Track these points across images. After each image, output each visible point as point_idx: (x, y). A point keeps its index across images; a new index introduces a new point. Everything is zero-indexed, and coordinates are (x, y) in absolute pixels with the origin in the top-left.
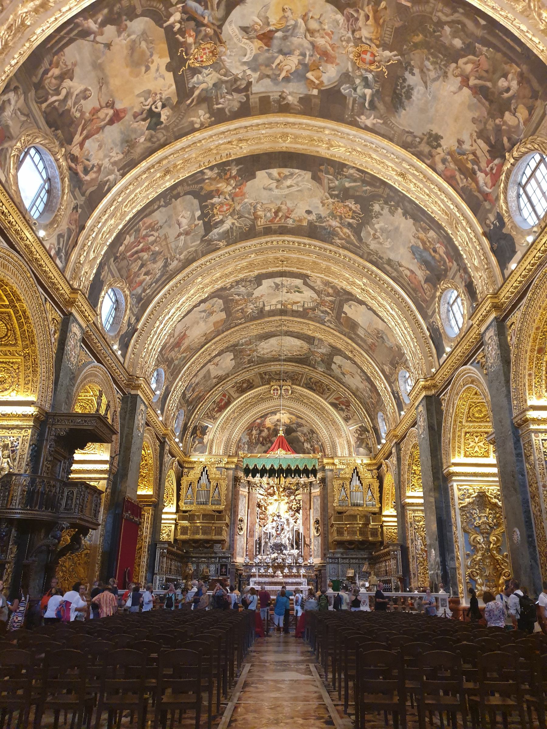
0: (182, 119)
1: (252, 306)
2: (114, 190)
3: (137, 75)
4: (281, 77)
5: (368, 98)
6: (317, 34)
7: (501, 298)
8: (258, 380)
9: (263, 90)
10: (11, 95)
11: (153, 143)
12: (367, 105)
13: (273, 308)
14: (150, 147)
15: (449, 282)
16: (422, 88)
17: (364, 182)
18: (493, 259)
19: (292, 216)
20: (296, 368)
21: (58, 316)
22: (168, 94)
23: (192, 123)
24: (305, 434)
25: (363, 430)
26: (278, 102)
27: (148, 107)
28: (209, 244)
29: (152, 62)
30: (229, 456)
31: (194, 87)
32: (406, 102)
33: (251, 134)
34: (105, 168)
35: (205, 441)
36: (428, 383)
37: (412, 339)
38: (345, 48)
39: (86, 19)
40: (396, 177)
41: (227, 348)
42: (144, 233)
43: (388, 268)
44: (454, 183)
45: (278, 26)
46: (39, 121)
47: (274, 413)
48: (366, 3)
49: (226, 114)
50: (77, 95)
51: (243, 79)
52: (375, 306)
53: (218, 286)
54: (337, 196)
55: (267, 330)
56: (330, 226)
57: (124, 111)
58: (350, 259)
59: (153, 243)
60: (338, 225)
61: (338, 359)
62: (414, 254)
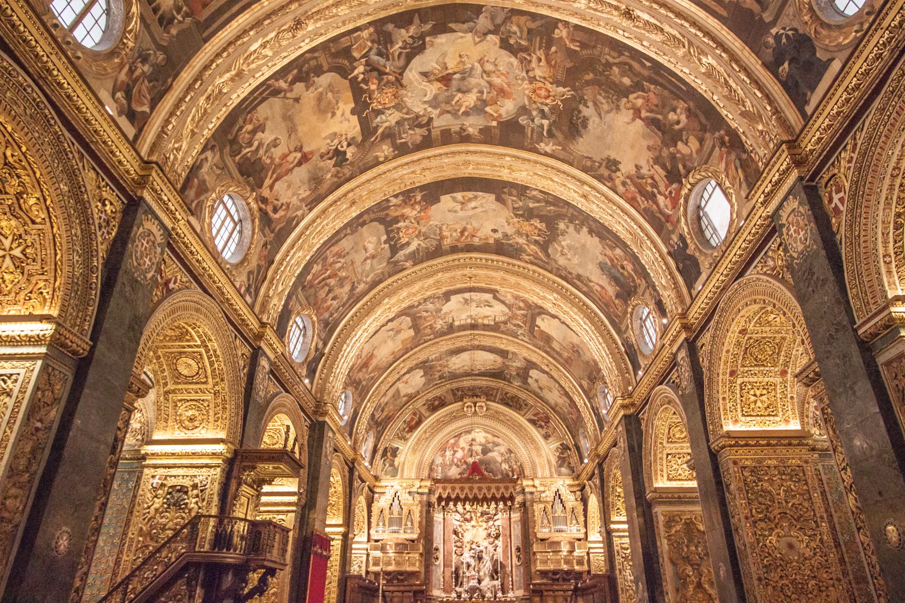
1: (441, 322)
2: (302, 224)
3: (324, 121)
4: (461, 112)
5: (545, 128)
7: (690, 317)
8: (450, 397)
9: (444, 123)
11: (339, 178)
12: (545, 133)
13: (463, 322)
15: (639, 299)
16: (597, 119)
17: (547, 202)
18: (680, 279)
19: (479, 234)
20: (490, 383)
21: (246, 350)
23: (377, 157)
24: (502, 454)
25: (565, 448)
26: (459, 133)
28: (395, 266)
29: (338, 108)
30: (422, 480)
32: (583, 131)
33: (434, 163)
35: (396, 463)
36: (627, 401)
37: (607, 355)
38: (520, 85)
40: (579, 199)
41: (417, 365)
42: (331, 260)
43: (578, 283)
44: (636, 204)
45: (456, 70)
47: (469, 432)
48: (537, 48)
51: (424, 116)
52: (568, 321)
53: (404, 305)
54: (521, 216)
55: (459, 344)
56: (517, 243)
57: (312, 153)
58: (539, 274)
59: (339, 269)
60: (525, 242)
61: (534, 373)
62: (602, 269)
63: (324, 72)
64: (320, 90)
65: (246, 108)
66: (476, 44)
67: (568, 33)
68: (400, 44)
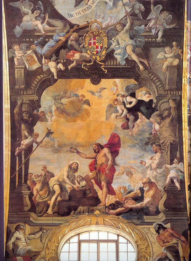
0: (158, 78)
3: (88, 114)
10: (17, 234)
14: (172, 120)
22: (122, 88)
23: (170, 67)
27: (125, 111)
29: (83, 96)
31: (127, 60)
34: (155, 177)
39: (19, 145)
46: (54, 222)
49: (174, 28)
50: (68, 177)
51: (133, 7)
63: (39, 101)
64: (54, 108)
65: (20, 182)
68: (38, 23)
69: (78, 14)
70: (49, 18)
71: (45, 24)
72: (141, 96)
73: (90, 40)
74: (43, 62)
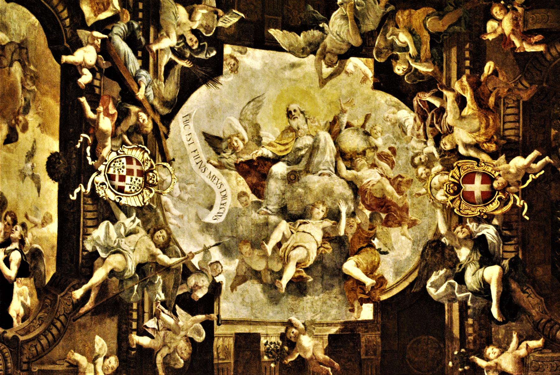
4: (284, 282)
6: (360, 161)
9: (244, 314)
31: (95, 255)
45: (279, 150)
66: (323, 82)
67: (515, 20)
69: (189, 138)
70: (183, 68)
71: (171, 56)
72: (20, 294)
73: (138, 163)
74: (96, 34)
